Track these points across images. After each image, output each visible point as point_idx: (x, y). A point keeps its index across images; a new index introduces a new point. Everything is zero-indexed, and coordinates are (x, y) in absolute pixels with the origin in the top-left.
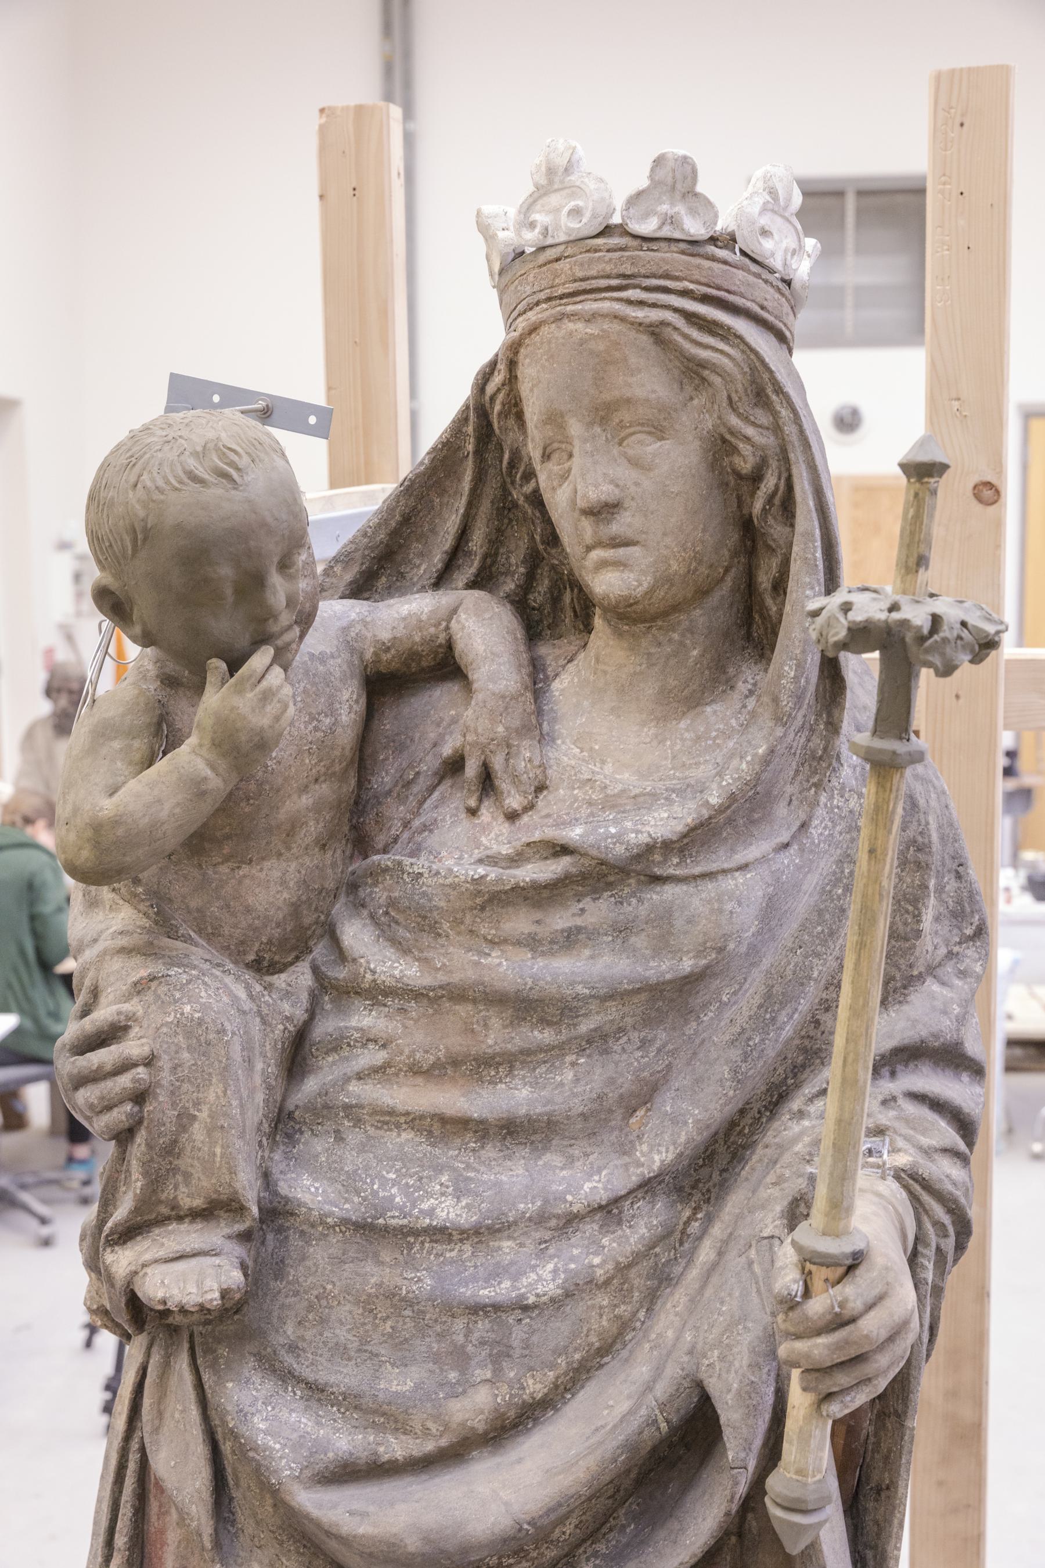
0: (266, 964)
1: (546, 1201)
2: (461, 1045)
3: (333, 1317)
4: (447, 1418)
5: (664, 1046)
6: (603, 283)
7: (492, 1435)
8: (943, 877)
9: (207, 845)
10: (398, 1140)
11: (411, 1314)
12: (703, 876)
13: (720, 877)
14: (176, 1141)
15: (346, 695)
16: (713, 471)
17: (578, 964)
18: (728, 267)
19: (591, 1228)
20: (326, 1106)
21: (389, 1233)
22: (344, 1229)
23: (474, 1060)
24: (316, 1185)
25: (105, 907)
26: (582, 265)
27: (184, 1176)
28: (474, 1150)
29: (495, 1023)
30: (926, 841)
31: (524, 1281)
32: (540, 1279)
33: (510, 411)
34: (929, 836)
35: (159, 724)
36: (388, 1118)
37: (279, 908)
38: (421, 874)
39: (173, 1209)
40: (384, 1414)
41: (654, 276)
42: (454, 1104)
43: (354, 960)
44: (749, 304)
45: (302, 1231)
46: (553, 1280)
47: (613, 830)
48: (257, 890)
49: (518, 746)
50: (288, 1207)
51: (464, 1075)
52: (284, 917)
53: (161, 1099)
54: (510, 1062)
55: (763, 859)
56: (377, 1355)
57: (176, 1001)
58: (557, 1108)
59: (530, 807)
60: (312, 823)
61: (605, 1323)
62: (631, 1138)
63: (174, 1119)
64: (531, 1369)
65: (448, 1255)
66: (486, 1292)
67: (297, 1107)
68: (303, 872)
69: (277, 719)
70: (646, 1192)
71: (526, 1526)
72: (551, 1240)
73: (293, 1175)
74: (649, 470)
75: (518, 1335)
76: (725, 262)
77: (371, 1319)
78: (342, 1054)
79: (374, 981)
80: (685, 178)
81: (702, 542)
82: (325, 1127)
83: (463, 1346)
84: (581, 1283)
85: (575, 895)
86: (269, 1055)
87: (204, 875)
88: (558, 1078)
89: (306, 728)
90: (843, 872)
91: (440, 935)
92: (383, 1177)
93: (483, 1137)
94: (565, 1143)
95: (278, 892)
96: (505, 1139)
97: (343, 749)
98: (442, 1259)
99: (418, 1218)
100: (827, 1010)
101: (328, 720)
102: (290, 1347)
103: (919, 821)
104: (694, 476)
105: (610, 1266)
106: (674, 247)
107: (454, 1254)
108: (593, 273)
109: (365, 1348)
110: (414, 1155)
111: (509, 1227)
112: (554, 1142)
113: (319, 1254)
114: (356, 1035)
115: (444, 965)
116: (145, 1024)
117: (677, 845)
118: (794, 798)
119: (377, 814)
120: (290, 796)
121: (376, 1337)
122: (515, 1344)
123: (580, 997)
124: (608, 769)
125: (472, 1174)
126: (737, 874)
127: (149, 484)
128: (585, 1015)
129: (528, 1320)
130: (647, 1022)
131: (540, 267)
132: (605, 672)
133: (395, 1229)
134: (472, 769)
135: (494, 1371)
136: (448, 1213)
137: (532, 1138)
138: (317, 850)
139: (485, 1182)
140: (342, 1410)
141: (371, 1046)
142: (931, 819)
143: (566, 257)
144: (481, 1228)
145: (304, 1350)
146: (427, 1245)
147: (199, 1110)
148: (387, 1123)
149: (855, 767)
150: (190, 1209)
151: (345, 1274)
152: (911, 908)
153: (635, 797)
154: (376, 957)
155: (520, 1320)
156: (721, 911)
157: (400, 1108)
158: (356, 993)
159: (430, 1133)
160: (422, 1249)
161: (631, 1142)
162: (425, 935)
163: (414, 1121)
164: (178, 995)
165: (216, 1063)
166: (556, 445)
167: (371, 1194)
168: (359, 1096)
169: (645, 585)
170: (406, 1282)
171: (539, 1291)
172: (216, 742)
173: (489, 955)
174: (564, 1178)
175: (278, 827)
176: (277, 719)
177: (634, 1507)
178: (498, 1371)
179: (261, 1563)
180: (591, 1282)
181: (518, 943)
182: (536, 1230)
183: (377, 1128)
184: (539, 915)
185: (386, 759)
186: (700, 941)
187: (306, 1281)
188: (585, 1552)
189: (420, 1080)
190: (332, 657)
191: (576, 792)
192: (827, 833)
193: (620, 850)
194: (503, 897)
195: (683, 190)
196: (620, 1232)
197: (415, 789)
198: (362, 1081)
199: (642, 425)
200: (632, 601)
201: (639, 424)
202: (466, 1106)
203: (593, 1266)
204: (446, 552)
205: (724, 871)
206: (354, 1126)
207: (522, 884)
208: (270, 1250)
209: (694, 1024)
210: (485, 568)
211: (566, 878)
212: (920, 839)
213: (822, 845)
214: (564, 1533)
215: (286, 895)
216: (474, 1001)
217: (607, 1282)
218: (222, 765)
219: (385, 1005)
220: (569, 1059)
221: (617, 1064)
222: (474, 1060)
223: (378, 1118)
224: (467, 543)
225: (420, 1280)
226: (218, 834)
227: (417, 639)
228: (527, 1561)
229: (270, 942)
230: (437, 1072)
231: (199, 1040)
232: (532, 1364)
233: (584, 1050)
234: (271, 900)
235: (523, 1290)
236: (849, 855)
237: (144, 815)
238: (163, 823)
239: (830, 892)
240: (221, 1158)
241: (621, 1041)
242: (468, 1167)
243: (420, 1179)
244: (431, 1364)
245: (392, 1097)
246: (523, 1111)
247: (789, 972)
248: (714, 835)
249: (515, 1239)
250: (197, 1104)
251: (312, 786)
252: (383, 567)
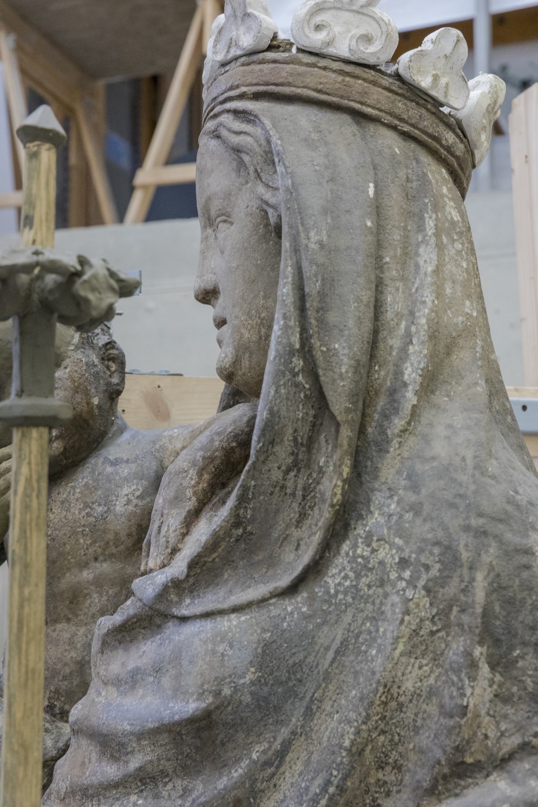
0: (57, 711)
5: (198, 797)
8: (512, 648)
12: (207, 615)
13: (219, 619)
15: (126, 490)
16: (267, 242)
18: (277, 65)
30: (470, 600)
34: (474, 595)
37: (66, 664)
44: (299, 91)
52: (71, 673)
55: (262, 602)
59: (164, 566)
76: (275, 61)
80: (240, 5)
81: (267, 308)
89: (80, 514)
90: (377, 631)
95: (66, 650)
100: (388, 794)
101: (100, 509)
103: (461, 576)
104: (246, 249)
106: (238, 64)
117: (184, 585)
118: (302, 543)
120: (69, 569)
126: (233, 616)
128: (132, 752)
142: (480, 576)
149: (390, 516)
152: (455, 679)
156: (214, 652)
169: (230, 356)
181: (113, 684)
186: (199, 682)
190: (127, 461)
192: (347, 583)
199: (218, 216)
205: (221, 612)
209: (225, 779)
212: (463, 598)
213: (341, 596)
215: (73, 654)
233: (142, 791)
234: (59, 656)
236: (383, 613)
239: (366, 652)
247: (325, 739)
248: (216, 576)
251: (93, 564)
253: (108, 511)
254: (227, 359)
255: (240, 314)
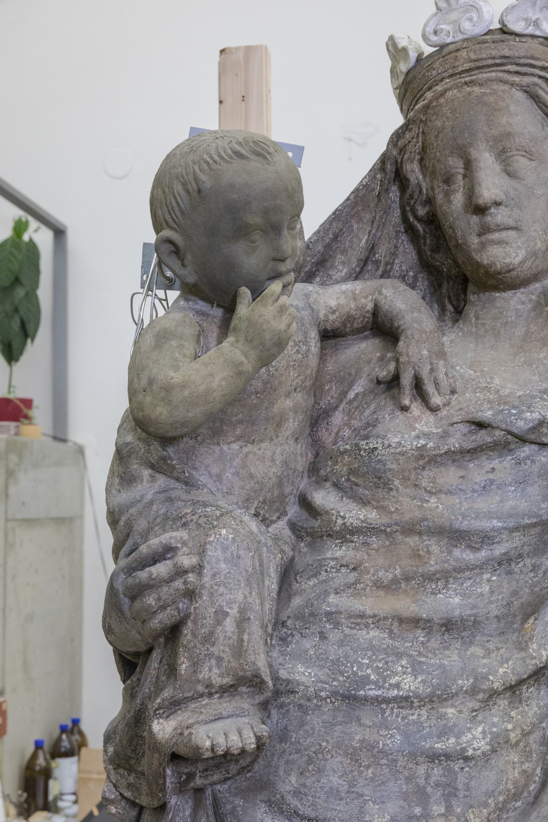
1: (476, 679)
2: (411, 566)
3: (328, 767)
6: (490, 62)
9: (225, 428)
10: (367, 636)
11: (386, 762)
14: (212, 633)
17: (492, 506)
19: (503, 703)
20: (312, 614)
21: (367, 701)
22: (333, 700)
23: (422, 576)
24: (308, 671)
25: (142, 481)
26: (475, 52)
27: (217, 660)
28: (422, 643)
29: (435, 549)
31: (464, 739)
32: (474, 738)
33: (414, 159)
35: (199, 336)
36: (360, 620)
37: (270, 478)
38: (376, 448)
39: (207, 687)
41: (524, 57)
42: (408, 608)
43: (327, 513)
45: (300, 705)
46: (484, 739)
47: (514, 412)
48: (257, 463)
49: (437, 364)
50: (288, 688)
51: (413, 588)
53: (204, 598)
54: (446, 578)
56: (362, 795)
57: (214, 527)
58: (480, 611)
59: (447, 404)
60: (291, 420)
61: (516, 775)
62: (525, 639)
63: (212, 615)
64: (472, 807)
65: (410, 718)
66: (439, 745)
67: (289, 617)
68: (285, 455)
69: (289, 326)
70: (535, 681)
72: (479, 710)
73: (290, 666)
74: (523, 179)
75: (461, 779)
77: (357, 767)
78: (321, 579)
79: (345, 524)
82: (311, 630)
83: (424, 788)
84: (502, 742)
85: (488, 459)
86: (273, 575)
87: (221, 450)
88: (479, 590)
91: (391, 489)
92: (359, 662)
93: (429, 633)
94: (484, 639)
95: (270, 466)
96: (444, 635)
97: (312, 370)
98: (406, 721)
99: (388, 689)
101: (304, 348)
102: (295, 792)
105: (519, 732)
106: (535, 41)
107: (415, 717)
108: (484, 56)
109: (353, 790)
110: (380, 646)
111: (453, 697)
112: (477, 638)
113: (315, 721)
114: (332, 563)
115: (397, 509)
116: (191, 544)
119: (327, 424)
121: (361, 782)
122: (460, 787)
123: (496, 528)
124: (497, 381)
125: (423, 659)
127: (208, 159)
128: (499, 542)
129: (468, 769)
130: (536, 552)
131: (444, 57)
132: (484, 324)
133: (372, 698)
134: (407, 380)
135: (446, 808)
136: (410, 686)
137: (463, 634)
138: (293, 441)
139: (433, 665)
141: (343, 570)
143: (463, 48)
144: (434, 697)
145: (305, 794)
146: (395, 710)
147: (231, 608)
148: (358, 624)
150: (221, 687)
151: (336, 734)
153: (519, 397)
154: (344, 509)
155: (462, 768)
157: (369, 612)
158: (329, 536)
159: (391, 632)
160: (392, 713)
161: (526, 642)
162: (380, 490)
163: (378, 621)
164: (215, 523)
165: (244, 571)
166: (453, 171)
167: (352, 674)
168: (337, 605)
170: (382, 738)
171: (475, 746)
172: (249, 339)
173: (428, 501)
174: (485, 664)
175: (273, 418)
176: (289, 326)
178: (449, 808)
180: (507, 742)
181: (449, 492)
182: (470, 701)
183: (351, 628)
184: (462, 473)
185: (331, 388)
187: (305, 741)
189: (381, 593)
191: (478, 395)
193: (521, 423)
194: (439, 460)
195: (541, 6)
196: (521, 709)
197: (355, 404)
198: (339, 595)
200: (511, 267)
201: (517, 150)
202: (417, 609)
203: (508, 730)
204: (361, 260)
206: (334, 628)
207: (453, 449)
208: (275, 720)
210: (386, 272)
211: (484, 445)
215: (274, 470)
216: (420, 534)
217: (517, 744)
218: (253, 355)
219: (352, 542)
220: (486, 576)
221: (518, 581)
222: (422, 576)
223: (352, 620)
224: (374, 255)
225: (392, 736)
226: (234, 419)
227: (353, 306)
229: (264, 502)
230: (394, 586)
231: (232, 555)
232: (472, 803)
233: (496, 570)
234: (266, 471)
235: (464, 745)
237: (202, 383)
238: (215, 391)
240: (248, 642)
241: (520, 565)
242: (420, 654)
243: (387, 663)
244: (402, 802)
245: (362, 605)
246: (457, 613)
249: (456, 708)
250: (230, 603)
252: (318, 270)
253: (308, 350)
254: (517, 258)
255: (539, 229)
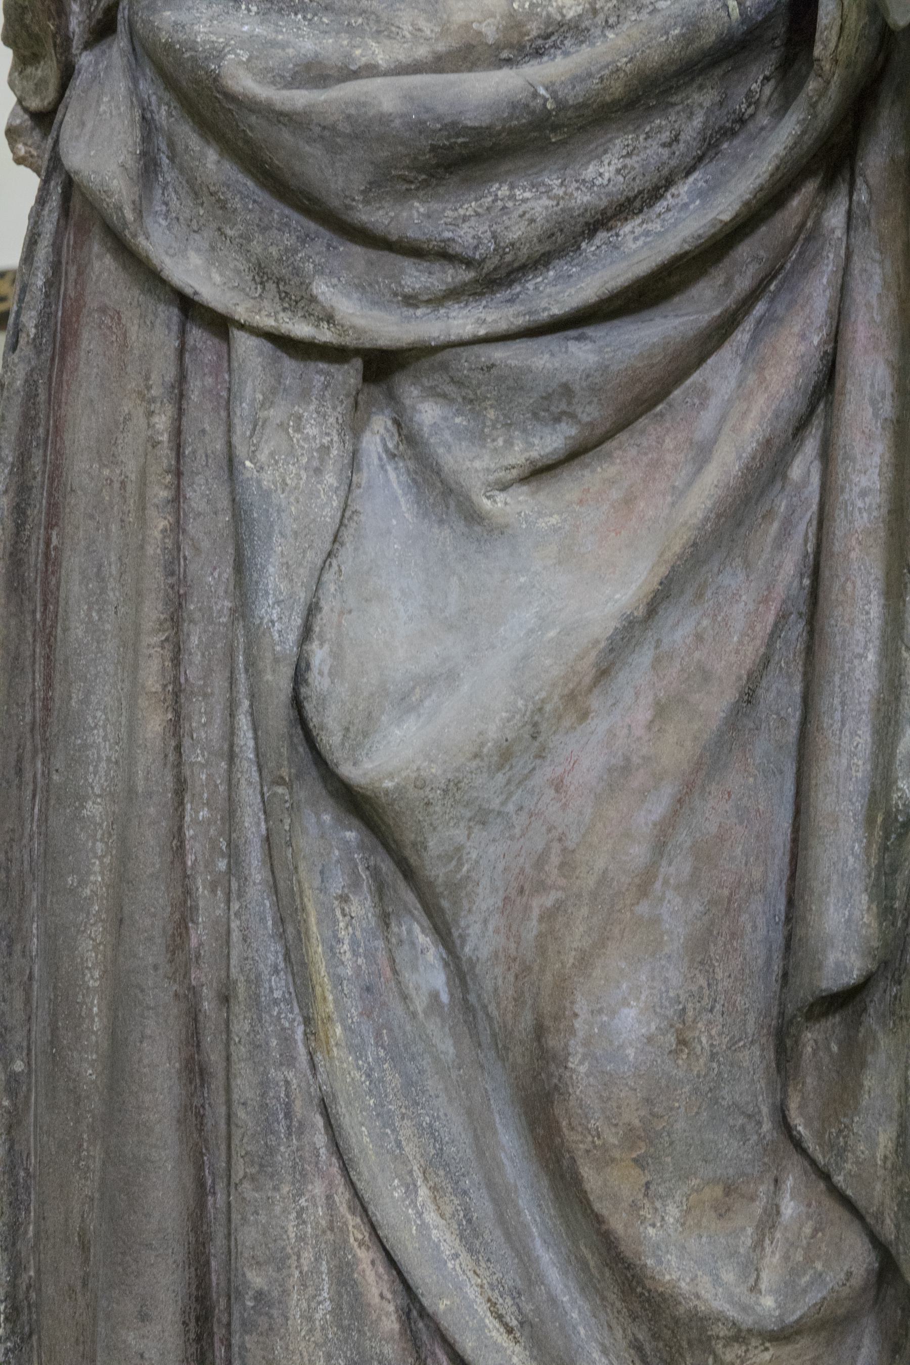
4: (445, 16)
7: (505, 54)
40: (363, 12)
71: (542, 91)
140: (309, 16)
177: (701, 184)
179: (198, 250)
188: (633, 232)
214: (601, 175)
228: (549, 198)
